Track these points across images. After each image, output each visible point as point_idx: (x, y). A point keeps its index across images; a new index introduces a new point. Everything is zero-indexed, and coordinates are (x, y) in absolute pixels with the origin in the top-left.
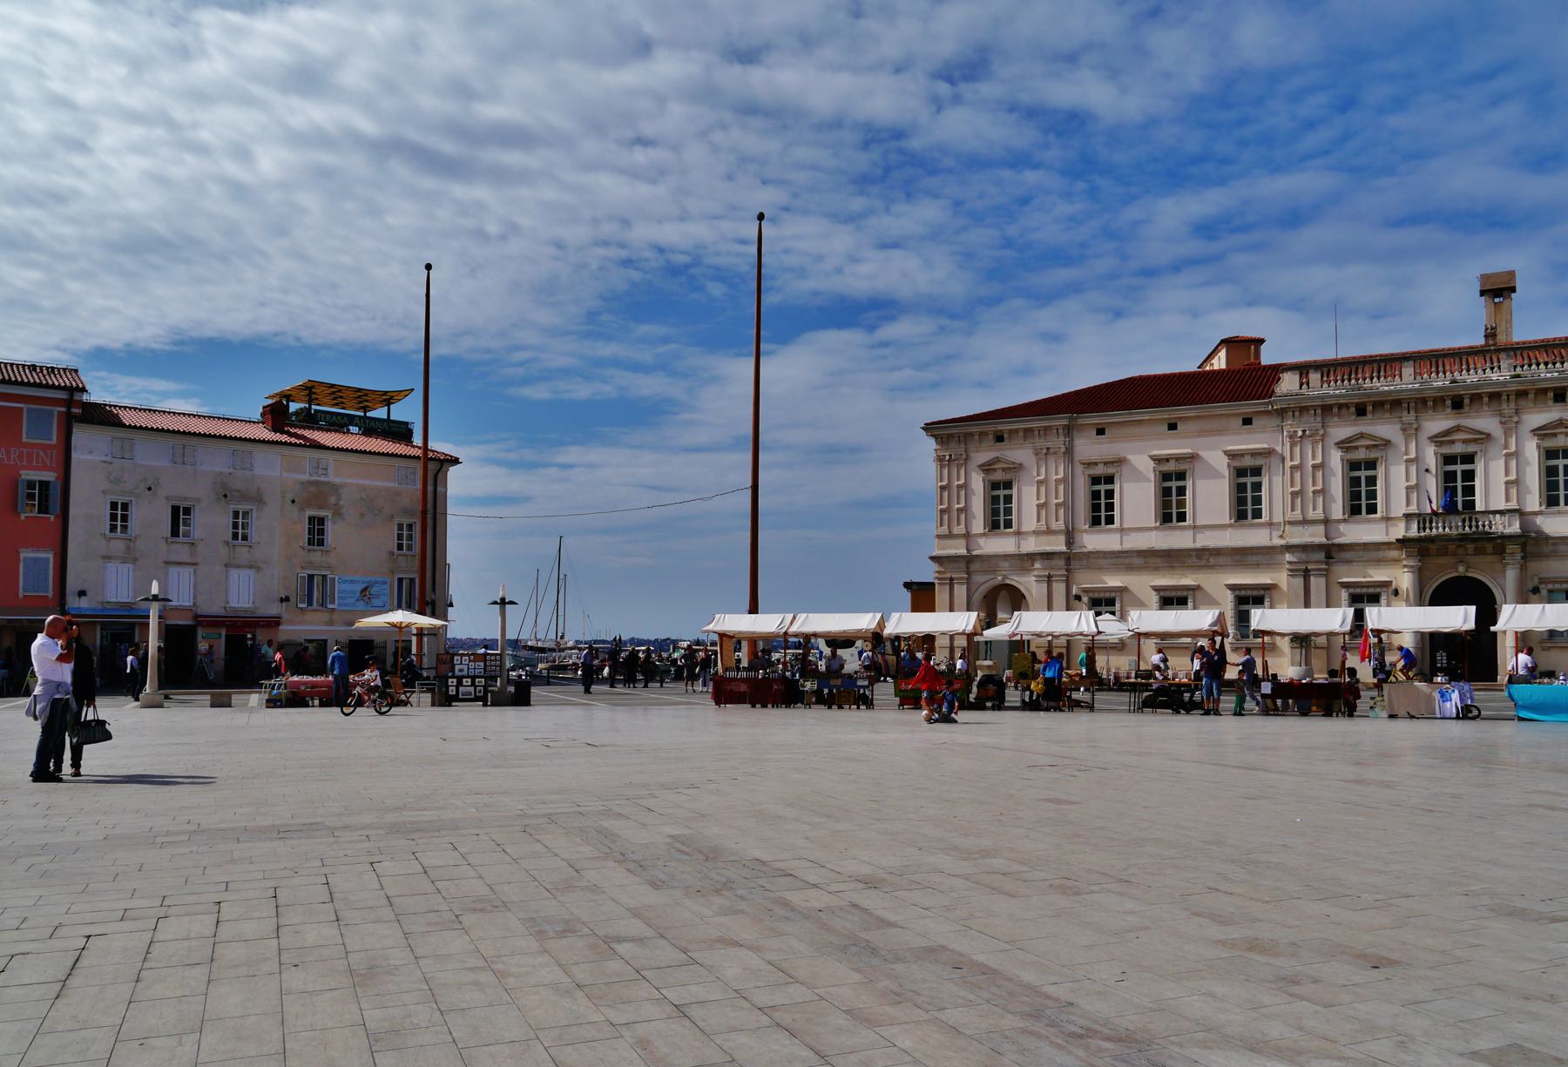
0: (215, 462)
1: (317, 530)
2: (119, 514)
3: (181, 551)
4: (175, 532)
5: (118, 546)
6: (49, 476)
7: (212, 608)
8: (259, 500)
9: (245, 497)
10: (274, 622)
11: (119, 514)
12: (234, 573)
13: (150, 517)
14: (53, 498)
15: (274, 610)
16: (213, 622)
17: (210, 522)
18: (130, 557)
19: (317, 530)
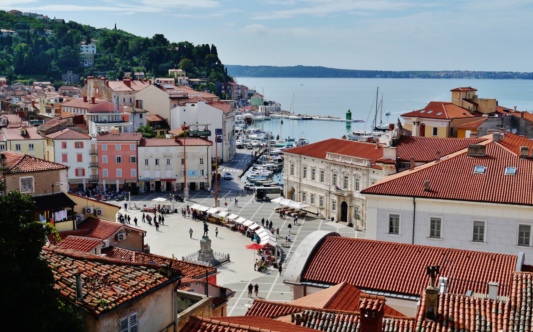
0: (163, 150)
1: (183, 162)
2: (147, 162)
3: (157, 167)
4: (156, 164)
5: (146, 167)
6: (135, 156)
7: (164, 178)
8: (171, 157)
9: (169, 157)
10: (175, 180)
11: (147, 162)
12: (167, 171)
13: (152, 162)
14: (135, 160)
15: (174, 177)
16: (164, 180)
17: (163, 162)
18: (149, 169)
19: (183, 162)
